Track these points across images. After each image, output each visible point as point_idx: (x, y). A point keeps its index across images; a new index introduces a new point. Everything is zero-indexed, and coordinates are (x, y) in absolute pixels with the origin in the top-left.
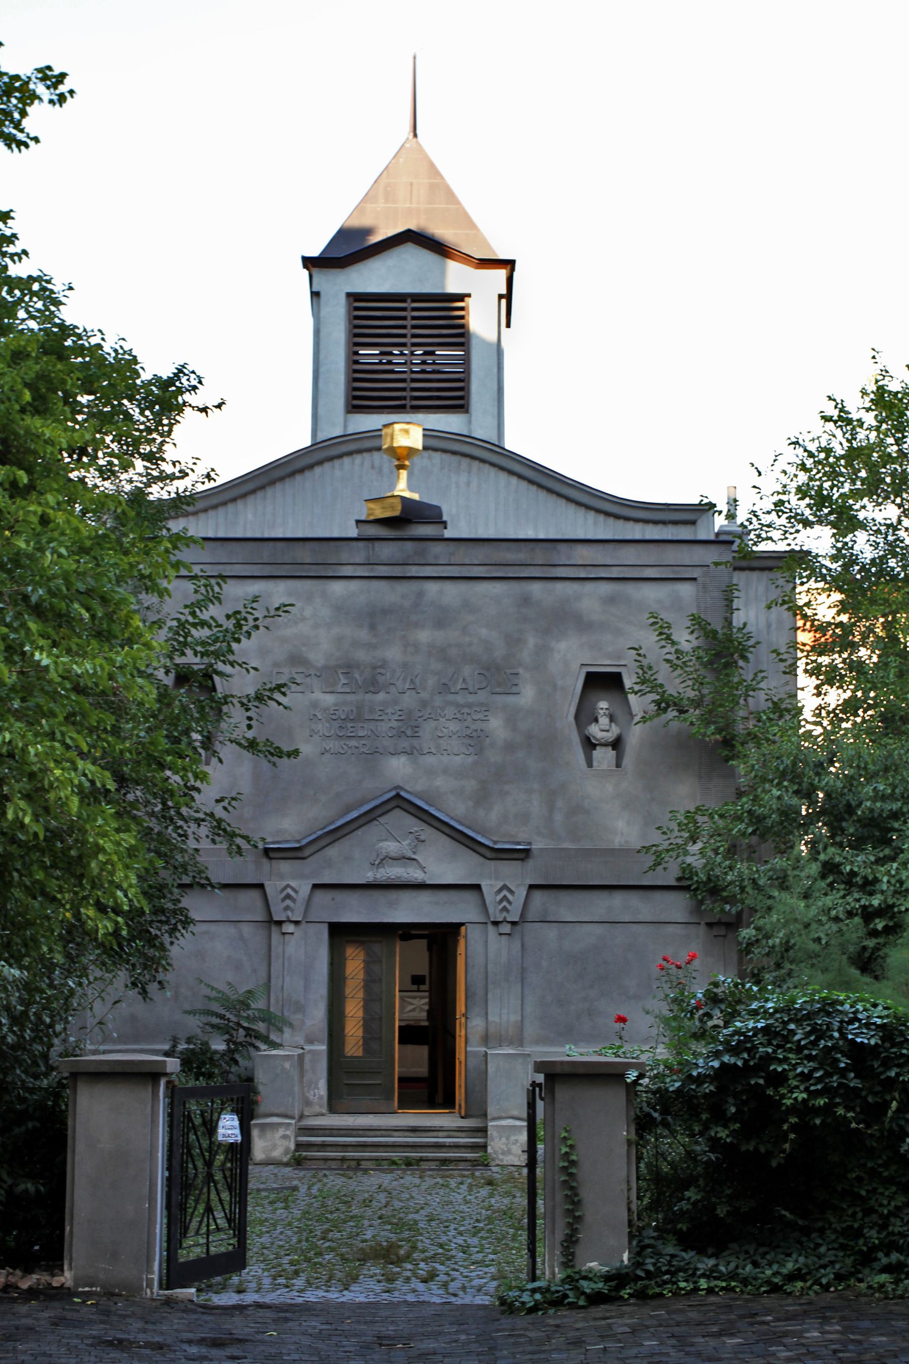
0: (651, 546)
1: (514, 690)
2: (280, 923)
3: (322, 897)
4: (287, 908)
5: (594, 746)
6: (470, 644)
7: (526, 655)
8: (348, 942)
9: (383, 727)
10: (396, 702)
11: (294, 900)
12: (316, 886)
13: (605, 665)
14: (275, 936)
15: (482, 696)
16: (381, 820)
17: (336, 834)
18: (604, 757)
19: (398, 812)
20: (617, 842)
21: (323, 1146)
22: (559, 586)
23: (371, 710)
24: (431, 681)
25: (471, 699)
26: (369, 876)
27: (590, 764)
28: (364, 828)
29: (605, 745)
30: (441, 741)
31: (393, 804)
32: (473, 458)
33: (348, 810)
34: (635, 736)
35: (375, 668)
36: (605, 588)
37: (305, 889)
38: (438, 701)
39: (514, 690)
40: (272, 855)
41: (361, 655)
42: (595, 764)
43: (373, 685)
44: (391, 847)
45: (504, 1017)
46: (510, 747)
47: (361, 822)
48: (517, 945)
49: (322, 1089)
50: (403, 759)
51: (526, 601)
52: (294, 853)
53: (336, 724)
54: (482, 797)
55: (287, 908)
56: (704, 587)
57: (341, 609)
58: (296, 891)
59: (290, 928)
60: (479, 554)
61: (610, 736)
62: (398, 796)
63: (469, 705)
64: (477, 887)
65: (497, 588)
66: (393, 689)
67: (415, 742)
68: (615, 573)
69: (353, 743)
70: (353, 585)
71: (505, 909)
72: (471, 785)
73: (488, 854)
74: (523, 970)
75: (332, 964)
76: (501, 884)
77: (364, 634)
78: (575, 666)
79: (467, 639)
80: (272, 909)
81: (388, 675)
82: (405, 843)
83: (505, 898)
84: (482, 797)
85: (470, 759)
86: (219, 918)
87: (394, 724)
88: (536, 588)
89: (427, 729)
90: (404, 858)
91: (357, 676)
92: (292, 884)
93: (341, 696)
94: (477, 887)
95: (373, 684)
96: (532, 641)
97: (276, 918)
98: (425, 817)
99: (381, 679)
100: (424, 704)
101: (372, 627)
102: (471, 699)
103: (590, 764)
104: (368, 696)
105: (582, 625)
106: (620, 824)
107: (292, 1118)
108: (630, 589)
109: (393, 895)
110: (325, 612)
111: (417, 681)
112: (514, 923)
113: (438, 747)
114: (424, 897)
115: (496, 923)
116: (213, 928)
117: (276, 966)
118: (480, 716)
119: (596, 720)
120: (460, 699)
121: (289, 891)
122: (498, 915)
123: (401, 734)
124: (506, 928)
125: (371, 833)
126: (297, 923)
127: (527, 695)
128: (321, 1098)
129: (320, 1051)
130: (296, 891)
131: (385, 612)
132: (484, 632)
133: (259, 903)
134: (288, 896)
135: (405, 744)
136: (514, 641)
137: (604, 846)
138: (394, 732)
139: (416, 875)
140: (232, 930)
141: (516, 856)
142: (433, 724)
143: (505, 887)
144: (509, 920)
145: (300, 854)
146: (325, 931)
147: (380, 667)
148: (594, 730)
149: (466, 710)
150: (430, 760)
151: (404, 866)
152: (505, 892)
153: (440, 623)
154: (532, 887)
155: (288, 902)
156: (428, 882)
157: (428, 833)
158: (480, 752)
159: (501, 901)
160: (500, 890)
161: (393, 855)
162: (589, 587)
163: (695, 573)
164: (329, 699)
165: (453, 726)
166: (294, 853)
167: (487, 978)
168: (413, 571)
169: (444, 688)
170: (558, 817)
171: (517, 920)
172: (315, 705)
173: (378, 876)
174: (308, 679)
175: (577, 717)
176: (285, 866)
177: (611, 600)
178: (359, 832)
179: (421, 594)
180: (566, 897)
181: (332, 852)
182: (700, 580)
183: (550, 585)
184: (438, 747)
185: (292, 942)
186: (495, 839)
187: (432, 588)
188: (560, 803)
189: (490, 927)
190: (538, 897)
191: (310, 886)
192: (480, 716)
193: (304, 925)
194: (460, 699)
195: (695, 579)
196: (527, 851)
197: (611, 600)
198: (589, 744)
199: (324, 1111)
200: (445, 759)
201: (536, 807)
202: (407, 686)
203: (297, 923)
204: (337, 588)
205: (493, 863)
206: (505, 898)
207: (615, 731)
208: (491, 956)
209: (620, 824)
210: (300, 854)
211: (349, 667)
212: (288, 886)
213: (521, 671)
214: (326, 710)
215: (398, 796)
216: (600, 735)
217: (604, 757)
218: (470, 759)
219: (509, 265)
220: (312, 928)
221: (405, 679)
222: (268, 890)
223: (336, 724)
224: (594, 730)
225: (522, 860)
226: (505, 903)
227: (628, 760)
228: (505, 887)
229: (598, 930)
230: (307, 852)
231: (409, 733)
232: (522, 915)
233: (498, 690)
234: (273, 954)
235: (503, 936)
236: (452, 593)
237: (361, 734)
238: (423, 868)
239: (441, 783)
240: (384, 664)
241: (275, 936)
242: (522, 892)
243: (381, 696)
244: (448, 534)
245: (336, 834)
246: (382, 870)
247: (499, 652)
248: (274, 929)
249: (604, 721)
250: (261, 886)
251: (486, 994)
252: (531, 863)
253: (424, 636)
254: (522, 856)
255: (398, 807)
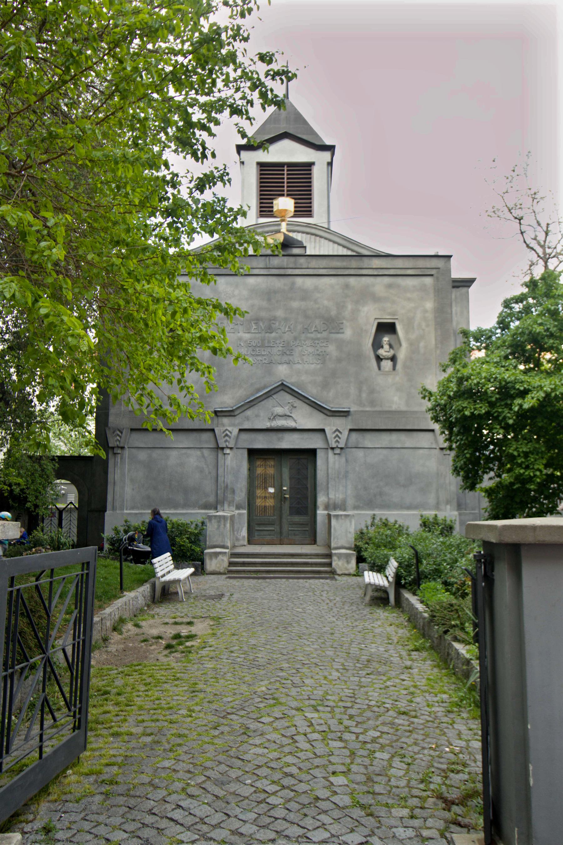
0: (411, 258)
1: (341, 331)
2: (223, 449)
3: (244, 436)
4: (226, 441)
5: (382, 359)
6: (319, 308)
7: (347, 313)
8: (257, 458)
9: (275, 350)
10: (281, 337)
11: (230, 437)
12: (241, 430)
13: (387, 319)
14: (220, 455)
15: (325, 334)
16: (275, 396)
17: (251, 404)
18: (387, 365)
19: (282, 393)
20: (394, 407)
21: (244, 564)
22: (364, 279)
23: (269, 342)
24: (299, 327)
25: (319, 336)
26: (267, 425)
27: (379, 368)
28: (265, 401)
29: (387, 359)
30: (304, 357)
31: (280, 388)
32: (316, 235)
33: (258, 390)
34: (402, 355)
35: (270, 320)
36: (387, 280)
37: (235, 431)
38: (303, 336)
39: (341, 331)
40: (218, 414)
41: (263, 314)
42: (382, 368)
43: (270, 329)
44: (279, 410)
45: (337, 496)
46: (339, 360)
47: (264, 397)
48: (343, 460)
49: (244, 533)
50: (285, 366)
51: (347, 286)
52: (230, 414)
53: (250, 349)
54: (325, 385)
55: (226, 441)
56: (437, 279)
57: (254, 291)
58: (231, 433)
59: (228, 451)
60: (324, 263)
61: (390, 354)
62: (282, 384)
63: (318, 339)
64: (323, 430)
65: (333, 280)
66: (279, 331)
67: (291, 358)
68: (392, 272)
69: (259, 358)
70: (260, 279)
71: (337, 441)
72: (319, 379)
73: (329, 413)
74: (347, 472)
75: (249, 469)
76: (335, 429)
77: (264, 304)
78: (372, 319)
79: (317, 306)
80: (219, 442)
81: (277, 324)
82: (286, 408)
83: (337, 436)
84: (325, 385)
85: (319, 366)
86: (192, 446)
87: (280, 349)
88: (352, 281)
89: (297, 350)
90: (286, 415)
91: (261, 324)
92: (230, 429)
93: (254, 335)
94: (323, 430)
95: (269, 329)
96: (349, 307)
97: (220, 446)
98: (296, 395)
99: (273, 326)
100: (295, 339)
101: (269, 300)
102: (319, 336)
103: (379, 368)
104: (267, 335)
105: (376, 299)
106: (396, 399)
107: (227, 548)
108: (399, 280)
109: (280, 435)
110: (245, 293)
111: (292, 327)
112: (341, 448)
113: (302, 360)
114: (296, 436)
115: (333, 449)
116: (189, 451)
117: (221, 471)
118: (324, 344)
119: (382, 347)
120: (312, 335)
121: (227, 432)
122: (333, 443)
123: (284, 353)
124: (338, 451)
125: (269, 403)
126: (231, 448)
127: (348, 333)
128: (244, 537)
129: (243, 514)
130: (231, 433)
131: (275, 292)
132: (326, 302)
133: (212, 439)
134: (227, 435)
135: (285, 358)
136: (341, 307)
137: (387, 409)
138: (281, 353)
139: (290, 424)
140: (198, 453)
141: (342, 414)
142: (300, 348)
143: (337, 430)
144: (339, 446)
145: (232, 414)
146: (245, 453)
147: (274, 320)
148: (381, 352)
149: (317, 342)
150: (299, 366)
151: (286, 419)
152: (337, 433)
153: (303, 299)
154: (351, 430)
155: (227, 438)
156: (298, 428)
157: (298, 403)
158: (324, 362)
159: (335, 437)
160: (335, 432)
161: (280, 414)
162: (379, 279)
163: (433, 272)
164: (247, 336)
165: (310, 350)
166: (230, 414)
167: (328, 476)
168: (289, 272)
169: (306, 330)
170: (364, 395)
171: (343, 446)
172: (240, 339)
173: (272, 425)
174: (236, 327)
175: (373, 345)
176: (225, 420)
177: (390, 286)
178: (263, 403)
179: (293, 283)
180: (368, 435)
181: (249, 413)
182: (435, 275)
183: (359, 279)
184: (302, 360)
185: (229, 458)
186: (332, 406)
187: (299, 281)
188: (365, 388)
189: (330, 451)
190: (354, 435)
191: (237, 430)
192: (324, 344)
193: (235, 450)
194: (312, 335)
195: (432, 275)
196: (348, 412)
197: (390, 286)
198: (379, 359)
199: (246, 543)
200: (306, 366)
201: (353, 390)
202: (287, 329)
203: (231, 448)
204: (251, 281)
205: (331, 418)
206: (337, 436)
207: (392, 353)
208: (331, 465)
209: (396, 399)
210: (232, 414)
211: (257, 320)
212: (227, 430)
213: (344, 322)
214: (246, 341)
215: (282, 384)
216: (385, 354)
217: (387, 365)
218: (319, 366)
219: (331, 149)
220: (240, 451)
221: (286, 326)
222: (216, 431)
223: (250, 349)
224: (381, 352)
225: (346, 416)
226: (337, 438)
227: (399, 366)
228: (337, 430)
229: (385, 452)
230: (236, 413)
231: (288, 353)
232: (346, 444)
233: (333, 331)
234: (219, 464)
235: (336, 456)
236: (309, 282)
237: (263, 353)
238: (295, 421)
239: (304, 378)
240: (275, 319)
241: (220, 455)
242: (346, 433)
243: (273, 335)
244: (308, 253)
245: (251, 404)
246: (274, 422)
247: (333, 313)
248: (220, 451)
249: (386, 347)
250: (213, 430)
251: (328, 484)
252: (350, 417)
253: (295, 304)
254: (345, 414)
255: (282, 390)
